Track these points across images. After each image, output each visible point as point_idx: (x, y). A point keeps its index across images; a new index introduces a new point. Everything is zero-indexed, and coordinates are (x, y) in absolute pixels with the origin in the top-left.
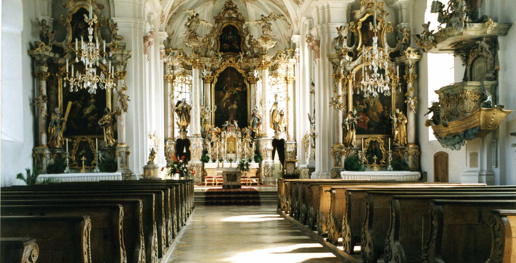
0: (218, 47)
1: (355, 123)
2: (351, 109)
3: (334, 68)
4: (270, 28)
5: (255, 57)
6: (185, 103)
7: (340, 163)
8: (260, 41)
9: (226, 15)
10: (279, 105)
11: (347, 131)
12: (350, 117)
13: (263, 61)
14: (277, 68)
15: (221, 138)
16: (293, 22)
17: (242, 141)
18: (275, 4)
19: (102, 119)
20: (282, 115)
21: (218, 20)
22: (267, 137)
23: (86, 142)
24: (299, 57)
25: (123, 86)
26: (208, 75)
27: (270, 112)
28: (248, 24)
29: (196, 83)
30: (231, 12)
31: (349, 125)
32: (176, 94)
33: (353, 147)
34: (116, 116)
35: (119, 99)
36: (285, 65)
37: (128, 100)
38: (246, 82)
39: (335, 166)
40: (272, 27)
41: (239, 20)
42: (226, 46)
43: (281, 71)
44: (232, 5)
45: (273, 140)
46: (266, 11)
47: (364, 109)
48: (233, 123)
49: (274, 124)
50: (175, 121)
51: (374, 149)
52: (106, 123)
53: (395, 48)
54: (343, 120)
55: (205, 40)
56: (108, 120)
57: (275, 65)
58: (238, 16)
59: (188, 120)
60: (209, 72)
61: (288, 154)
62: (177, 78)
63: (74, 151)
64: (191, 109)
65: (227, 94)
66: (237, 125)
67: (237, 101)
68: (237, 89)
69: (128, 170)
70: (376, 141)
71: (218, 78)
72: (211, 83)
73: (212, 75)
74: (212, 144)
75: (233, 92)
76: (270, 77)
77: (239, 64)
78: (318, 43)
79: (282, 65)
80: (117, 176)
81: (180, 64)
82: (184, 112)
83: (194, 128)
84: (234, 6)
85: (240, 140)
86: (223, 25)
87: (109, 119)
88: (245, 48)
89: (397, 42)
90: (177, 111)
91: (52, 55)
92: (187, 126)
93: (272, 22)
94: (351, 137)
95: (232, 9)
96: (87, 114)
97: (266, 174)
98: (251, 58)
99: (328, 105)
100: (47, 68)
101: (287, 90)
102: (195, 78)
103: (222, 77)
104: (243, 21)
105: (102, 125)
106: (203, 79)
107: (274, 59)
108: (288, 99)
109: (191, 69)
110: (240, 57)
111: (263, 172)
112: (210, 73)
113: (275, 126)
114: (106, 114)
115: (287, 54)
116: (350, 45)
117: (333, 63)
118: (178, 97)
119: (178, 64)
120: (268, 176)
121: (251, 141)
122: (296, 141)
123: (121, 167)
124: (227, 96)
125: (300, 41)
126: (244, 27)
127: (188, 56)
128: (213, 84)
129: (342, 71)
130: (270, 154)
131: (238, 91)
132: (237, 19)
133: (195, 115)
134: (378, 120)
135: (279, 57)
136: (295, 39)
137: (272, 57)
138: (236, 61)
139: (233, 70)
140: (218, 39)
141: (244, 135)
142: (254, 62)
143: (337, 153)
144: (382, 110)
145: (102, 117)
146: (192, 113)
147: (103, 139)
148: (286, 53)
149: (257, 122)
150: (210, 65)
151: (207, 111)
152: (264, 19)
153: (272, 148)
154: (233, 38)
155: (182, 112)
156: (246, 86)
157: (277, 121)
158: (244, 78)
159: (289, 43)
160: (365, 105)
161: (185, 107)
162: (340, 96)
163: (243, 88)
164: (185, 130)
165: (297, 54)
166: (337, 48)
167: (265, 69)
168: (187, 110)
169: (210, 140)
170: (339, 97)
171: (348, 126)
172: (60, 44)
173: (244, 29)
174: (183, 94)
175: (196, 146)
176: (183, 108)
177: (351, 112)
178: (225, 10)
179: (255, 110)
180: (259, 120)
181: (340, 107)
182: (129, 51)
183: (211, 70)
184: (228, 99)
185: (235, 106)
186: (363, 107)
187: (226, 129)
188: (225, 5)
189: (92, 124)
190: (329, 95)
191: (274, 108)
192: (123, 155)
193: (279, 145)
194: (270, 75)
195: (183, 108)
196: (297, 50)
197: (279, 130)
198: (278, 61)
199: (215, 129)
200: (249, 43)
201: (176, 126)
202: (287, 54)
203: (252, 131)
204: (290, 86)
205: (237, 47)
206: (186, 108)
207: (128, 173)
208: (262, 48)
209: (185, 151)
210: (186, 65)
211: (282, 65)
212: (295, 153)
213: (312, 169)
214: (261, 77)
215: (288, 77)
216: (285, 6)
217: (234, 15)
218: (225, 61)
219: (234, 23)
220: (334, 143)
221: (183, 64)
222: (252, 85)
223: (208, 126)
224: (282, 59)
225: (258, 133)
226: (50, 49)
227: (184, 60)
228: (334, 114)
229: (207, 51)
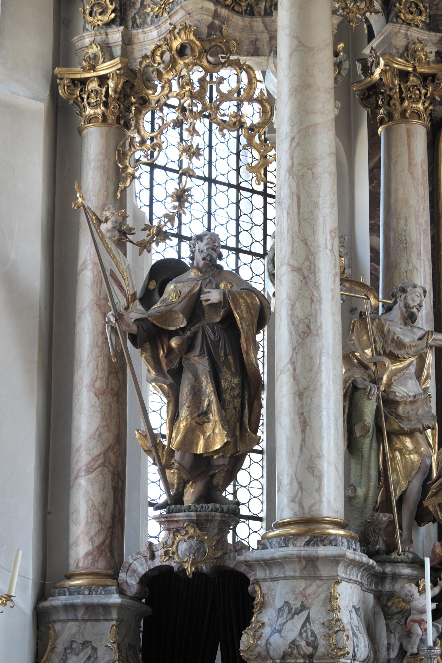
6: (211, 269)
29: (304, 133)
60: (415, 33)
64: (262, 316)
82: (203, 333)
83: (289, 480)
90: (150, 335)
102: (303, 88)
133: (305, 367)
146: (273, 351)
151: (408, 337)
155: (189, 346)
161: (214, 296)
168: (229, 321)
176: (195, 308)
206: (224, 303)
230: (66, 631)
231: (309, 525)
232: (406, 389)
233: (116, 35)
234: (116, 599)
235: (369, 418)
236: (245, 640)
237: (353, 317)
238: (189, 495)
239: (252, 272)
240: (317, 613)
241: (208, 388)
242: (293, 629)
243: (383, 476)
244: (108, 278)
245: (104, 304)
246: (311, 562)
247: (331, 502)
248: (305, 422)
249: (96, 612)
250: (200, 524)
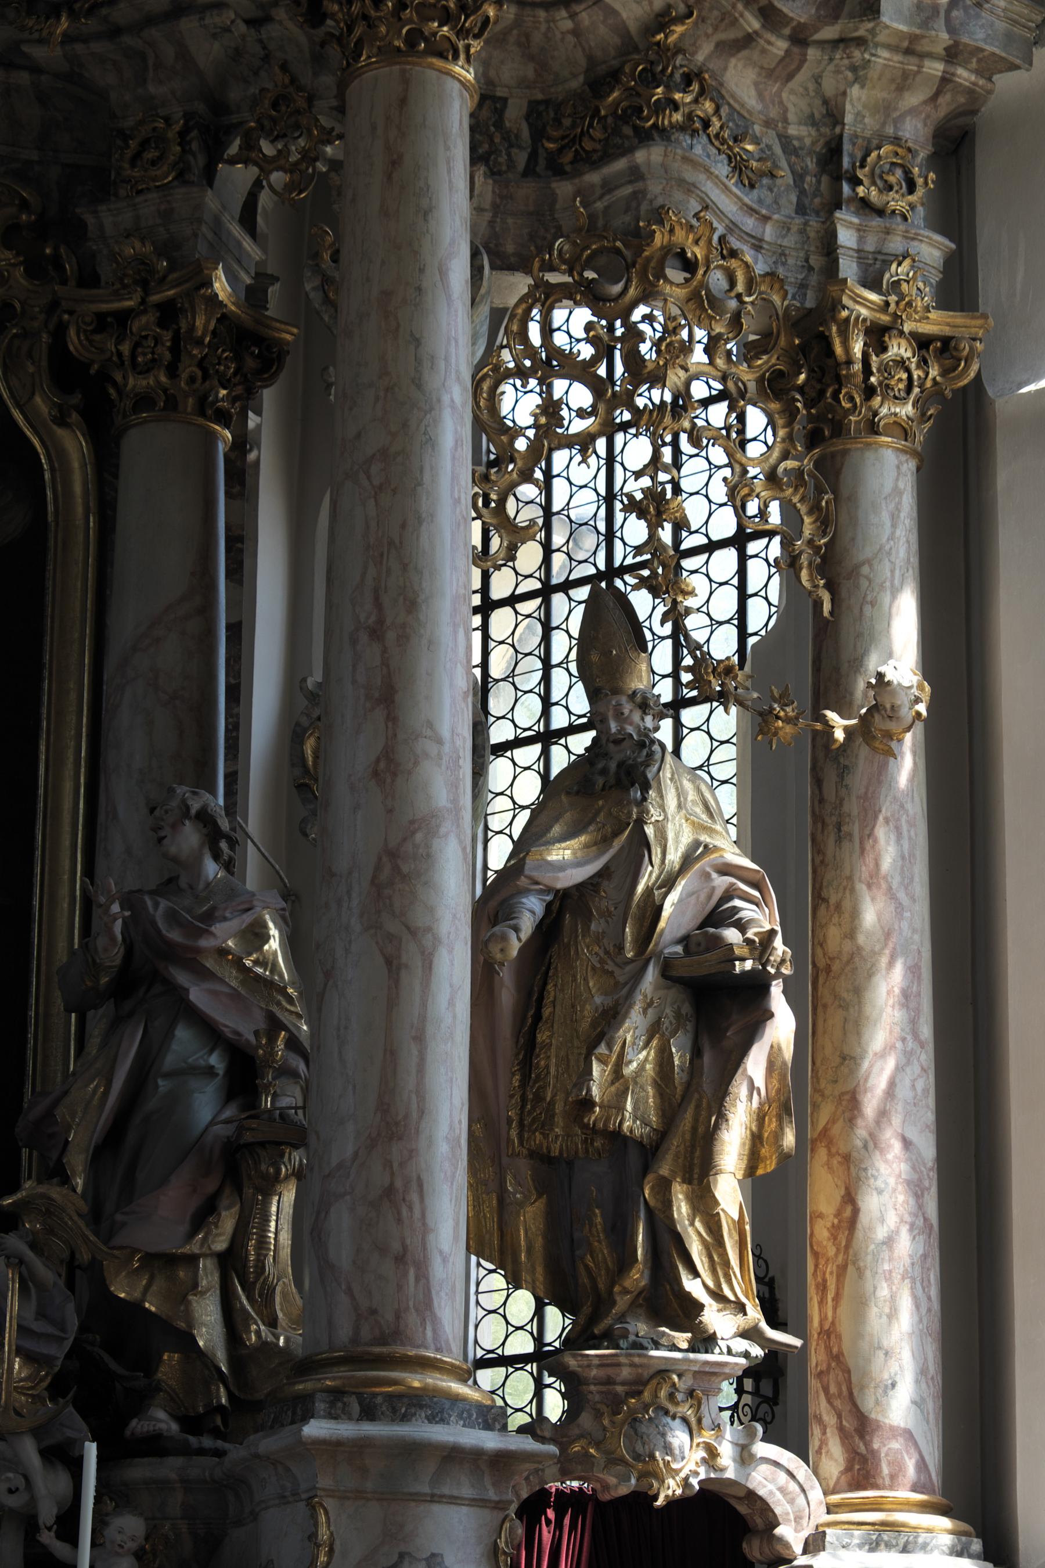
14: (636, 127)
36: (795, 100)
43: (716, 200)
49: (553, 1173)
57: (600, 82)
79: (741, 81)
113: (590, 1219)
149: (206, 1108)
157: (634, 1118)
179: (173, 881)
180: (244, 1074)
191: (566, 858)
203: (83, 1275)
204: (889, 485)
215: (863, 304)
222: (149, 449)
225: (208, 1330)
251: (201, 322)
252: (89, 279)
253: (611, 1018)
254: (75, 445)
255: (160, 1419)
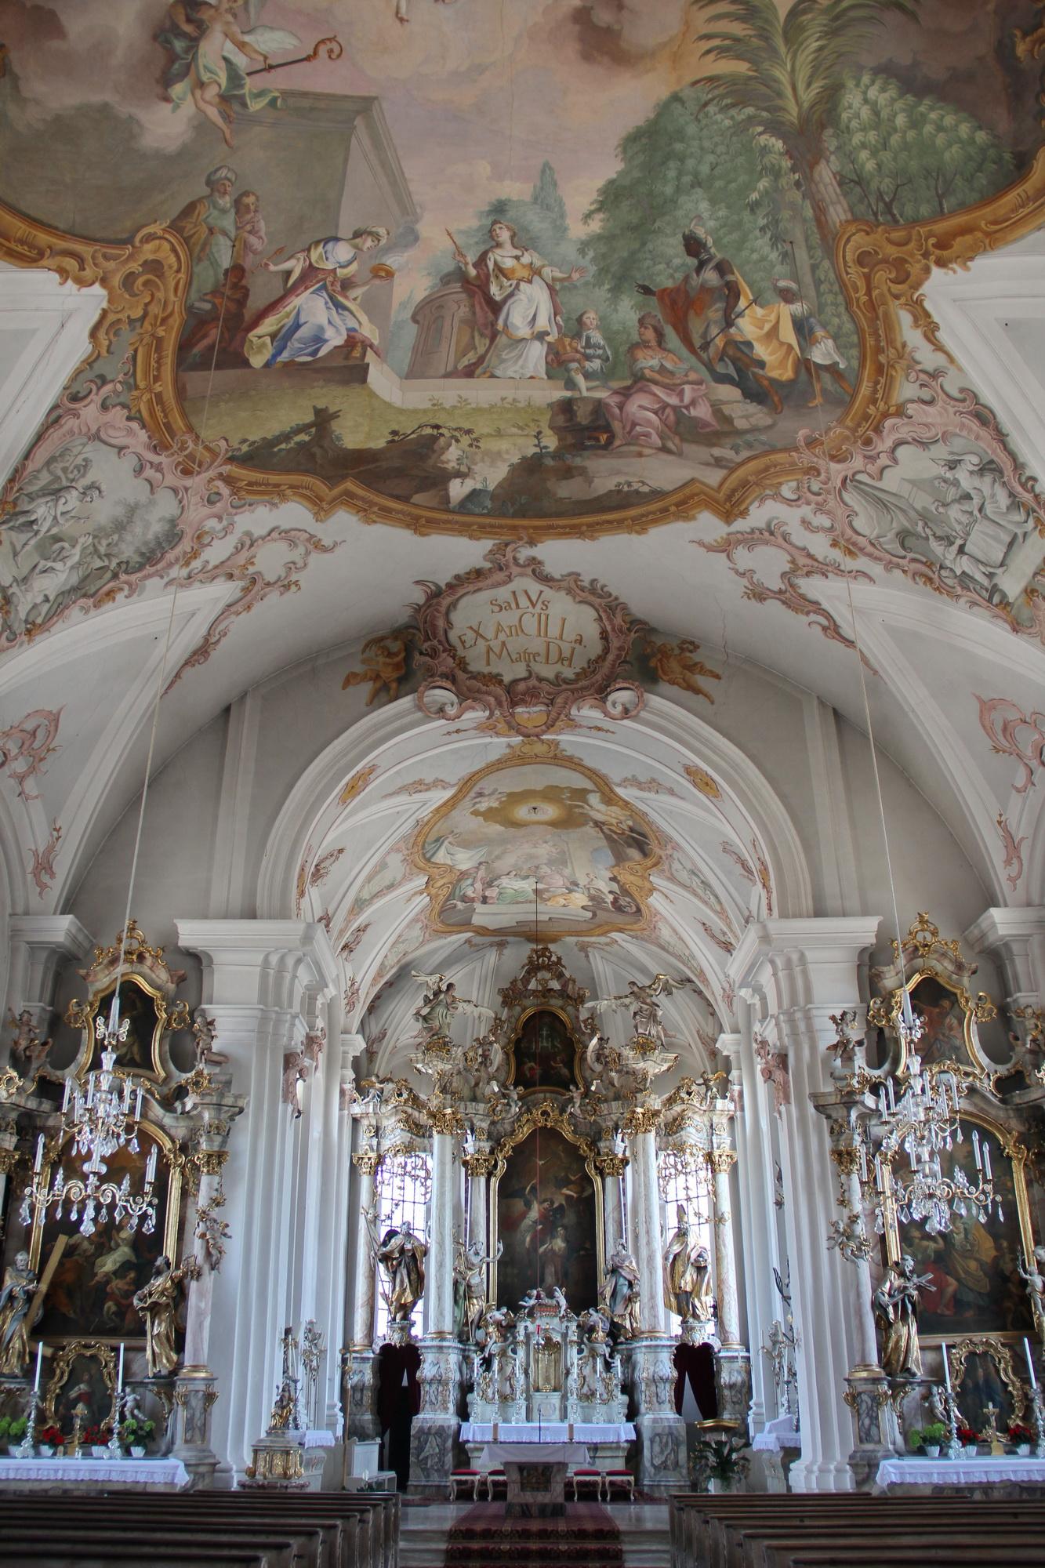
0: (508, 1073)
1: (910, 1296)
2: (894, 1255)
3: (832, 1132)
4: (655, 1016)
5: (617, 1098)
6: (408, 1235)
7: (874, 1430)
8: (628, 1053)
9: (533, 985)
10: (692, 1240)
11: (890, 1325)
12: (894, 1280)
13: (639, 1110)
15: (515, 1343)
16: (719, 999)
17: (580, 1351)
18: (668, 952)
19: (146, 1290)
20: (701, 1270)
21: (510, 996)
22: (657, 1338)
23: (94, 1358)
24: (741, 1094)
25: (214, 1194)
26: (478, 1151)
27: (666, 1258)
28: (594, 1009)
29: (442, 1177)
30: (547, 975)
31: (895, 1306)
32: (385, 1208)
33: (914, 1375)
34: (186, 1281)
35: (199, 1231)
36: (706, 1119)
37: (225, 1235)
38: (591, 1172)
39: (861, 1441)
40: (660, 1013)
41: (569, 997)
42: (531, 1069)
43: (694, 1135)
44: (549, 958)
45: (677, 1348)
46: (644, 970)
47: (937, 1253)
48: (551, 1295)
49: (677, 1296)
50: (380, 1289)
51: (981, 1381)
52: (155, 1304)
53: (1009, 1066)
54: (874, 1291)
55: (471, 1054)
56: (162, 1294)
57: (675, 1120)
58: (565, 986)
59: (418, 1283)
60: (482, 1144)
61: (726, 1392)
62: (388, 1161)
63: (55, 1388)
64: (425, 1253)
65: (535, 1206)
66: (563, 1302)
67: (565, 1228)
68: (565, 1191)
69: (205, 1451)
70: (985, 1353)
71: (509, 1160)
72: (490, 1175)
73: (492, 1152)
74: (487, 1363)
75: (552, 1203)
76: (662, 1154)
77: (569, 1116)
78: (782, 1059)
80: (167, 1472)
81: (400, 1121)
82: (406, 1261)
84: (554, 958)
85: (575, 1350)
86: (524, 1010)
87: (166, 1289)
88: (588, 1074)
89: (1012, 1048)
90: (386, 1258)
91: (32, 1104)
92: (414, 1303)
93: (661, 999)
94: (903, 1343)
95: (548, 968)
96: (107, 1274)
97: (657, 1462)
98: (606, 1101)
99: (824, 1244)
100: (15, 1139)
101: (715, 1193)
102: (442, 1163)
103: (520, 1157)
104: (580, 1000)
105: (142, 1309)
106: (465, 1163)
107: (670, 1101)
108: (717, 1220)
109: (431, 1136)
110: (571, 1100)
111: (646, 1453)
112: (486, 1146)
114: (159, 1273)
115: (708, 1088)
116: (876, 1062)
117: (829, 1117)
118: (389, 1218)
119: (393, 1119)
120: (664, 1466)
121: (607, 1351)
122: (748, 1350)
123: (186, 1441)
124: (534, 1213)
125: (741, 1049)
126: (584, 1015)
127: (423, 1097)
128: (493, 1179)
129: (858, 1139)
130: (667, 1392)
131: (568, 1197)
132: (563, 994)
133: (439, 1273)
134: (985, 1285)
135: (686, 1097)
136: (726, 1043)
137: (667, 1096)
138: (562, 1111)
139: (553, 1134)
140: (511, 1049)
141: (587, 1330)
142: (614, 1111)
143: (864, 1397)
144: (993, 1253)
145: (148, 1282)
147: (144, 1349)
148: (706, 1082)
149: (626, 1290)
150: (485, 1125)
151: (475, 1260)
152: (638, 992)
153: (675, 1374)
154: (554, 1046)
155: (399, 1264)
156: (591, 1182)
157: (688, 1289)
158: (584, 1159)
159: (714, 1054)
160: (940, 1241)
162: (857, 1217)
163: (583, 1190)
164: (405, 1317)
165: (736, 1088)
166: (837, 1073)
167: (647, 1131)
168: (414, 1255)
169: (482, 1350)
170: (853, 1219)
171: (891, 1309)
172: (59, 1073)
173: (585, 1021)
174: (408, 1206)
175: (439, 1366)
176: (402, 1251)
177: (897, 1264)
178: (528, 972)
180: (631, 1285)
181: (859, 1249)
182: (238, 1097)
183: (489, 1138)
184: (535, 1222)
185: (559, 1244)
186: (932, 1245)
187: (531, 1314)
188: (530, 957)
189: (117, 1304)
190: (827, 1214)
191: (676, 1249)
192: (196, 1403)
193: (695, 1363)
194: (660, 1149)
195: (402, 1251)
196: (734, 1075)
197: (696, 1316)
198: (684, 1107)
199: (498, 1315)
200: (598, 1059)
201: (381, 1303)
202: (708, 1088)
204: (724, 1179)
205: (565, 1071)
207: (206, 1465)
208: (634, 1073)
209: (405, 1383)
210: (417, 1125)
211: (696, 1117)
212: (746, 1389)
213: (792, 1453)
214: (634, 1155)
215: (716, 1153)
216: (694, 957)
217: (555, 985)
218: (529, 1111)
219: (555, 1003)
220: (853, 1366)
221: (407, 1121)
222: (609, 1180)
223: (476, 1307)
224: (696, 1103)
225: (628, 1326)
226: (32, 1087)
227: (410, 1110)
228: (844, 1271)
229: (477, 1084)
230: (352, 1365)
231: (440, 1335)
232: (475, 1281)
233: (375, 1142)
234: (372, 1355)
235: (462, 1293)
236: (418, 1374)
237: (457, 1255)
238: (399, 1316)
239: (420, 1236)
240: (442, 1365)
241: (406, 1280)
242: (434, 1371)
243: (466, 1315)
244: (372, 1240)
245: (370, 1247)
246: (441, 1347)
247: (448, 1326)
248: (440, 1298)
249: (364, 1360)
250: (402, 1329)
251: (617, 1162)
252: (599, 1154)
253: (684, 1272)
254: (599, 1179)
255: (622, 1339)
